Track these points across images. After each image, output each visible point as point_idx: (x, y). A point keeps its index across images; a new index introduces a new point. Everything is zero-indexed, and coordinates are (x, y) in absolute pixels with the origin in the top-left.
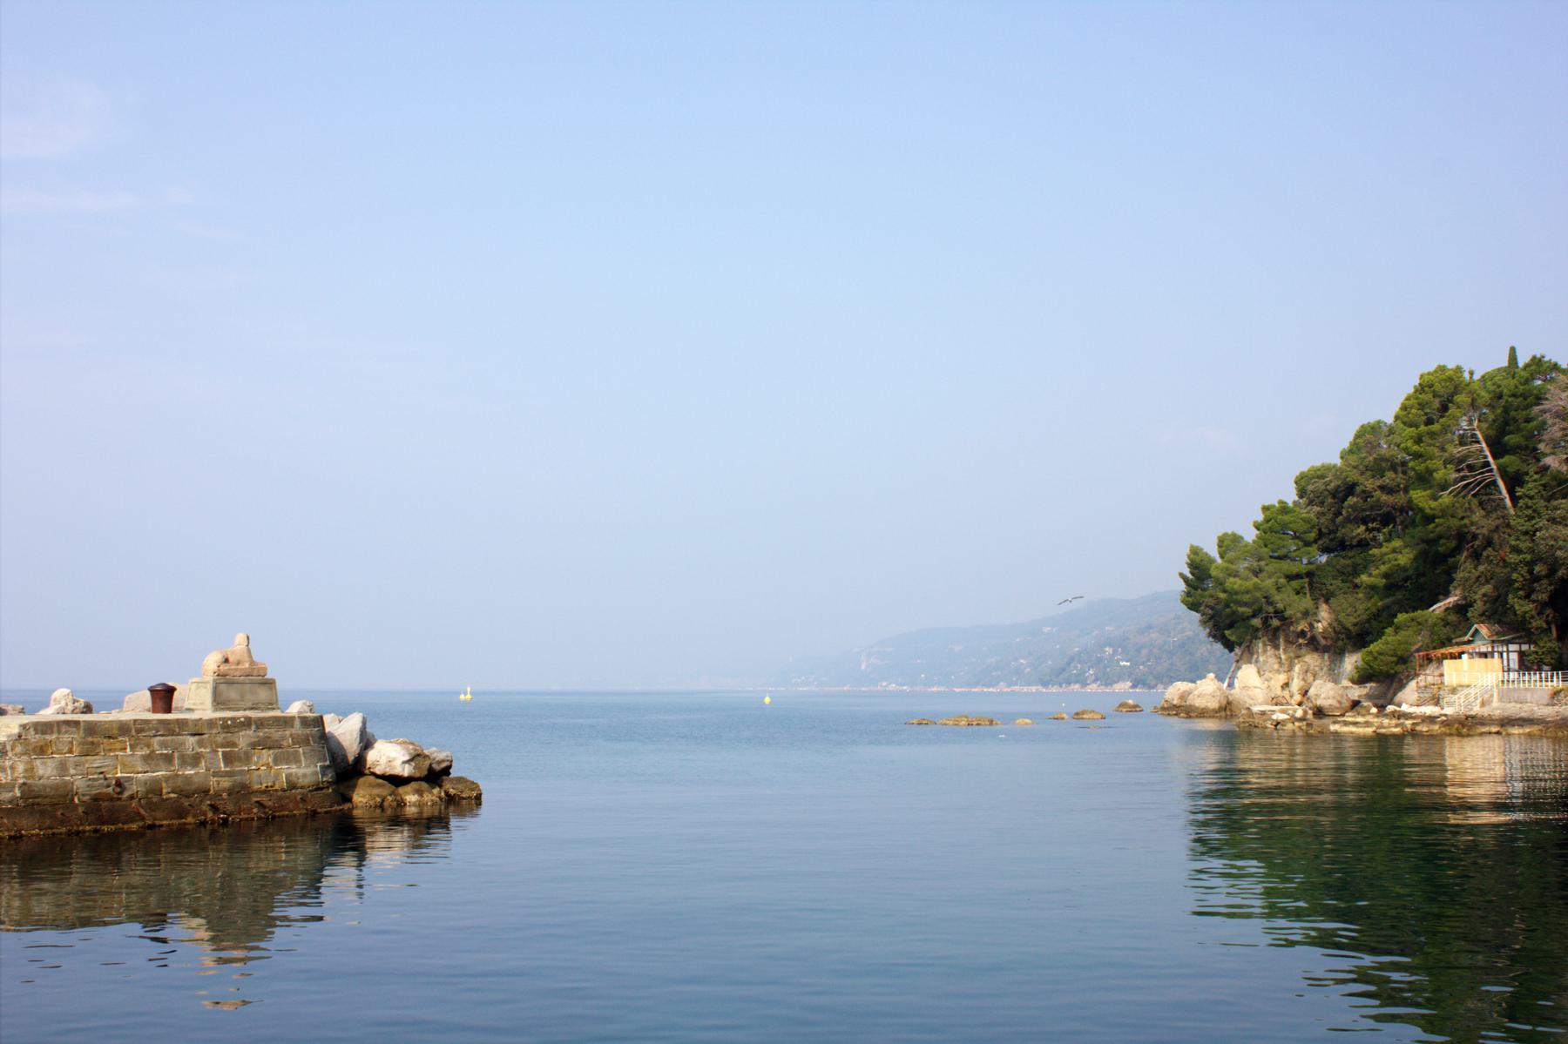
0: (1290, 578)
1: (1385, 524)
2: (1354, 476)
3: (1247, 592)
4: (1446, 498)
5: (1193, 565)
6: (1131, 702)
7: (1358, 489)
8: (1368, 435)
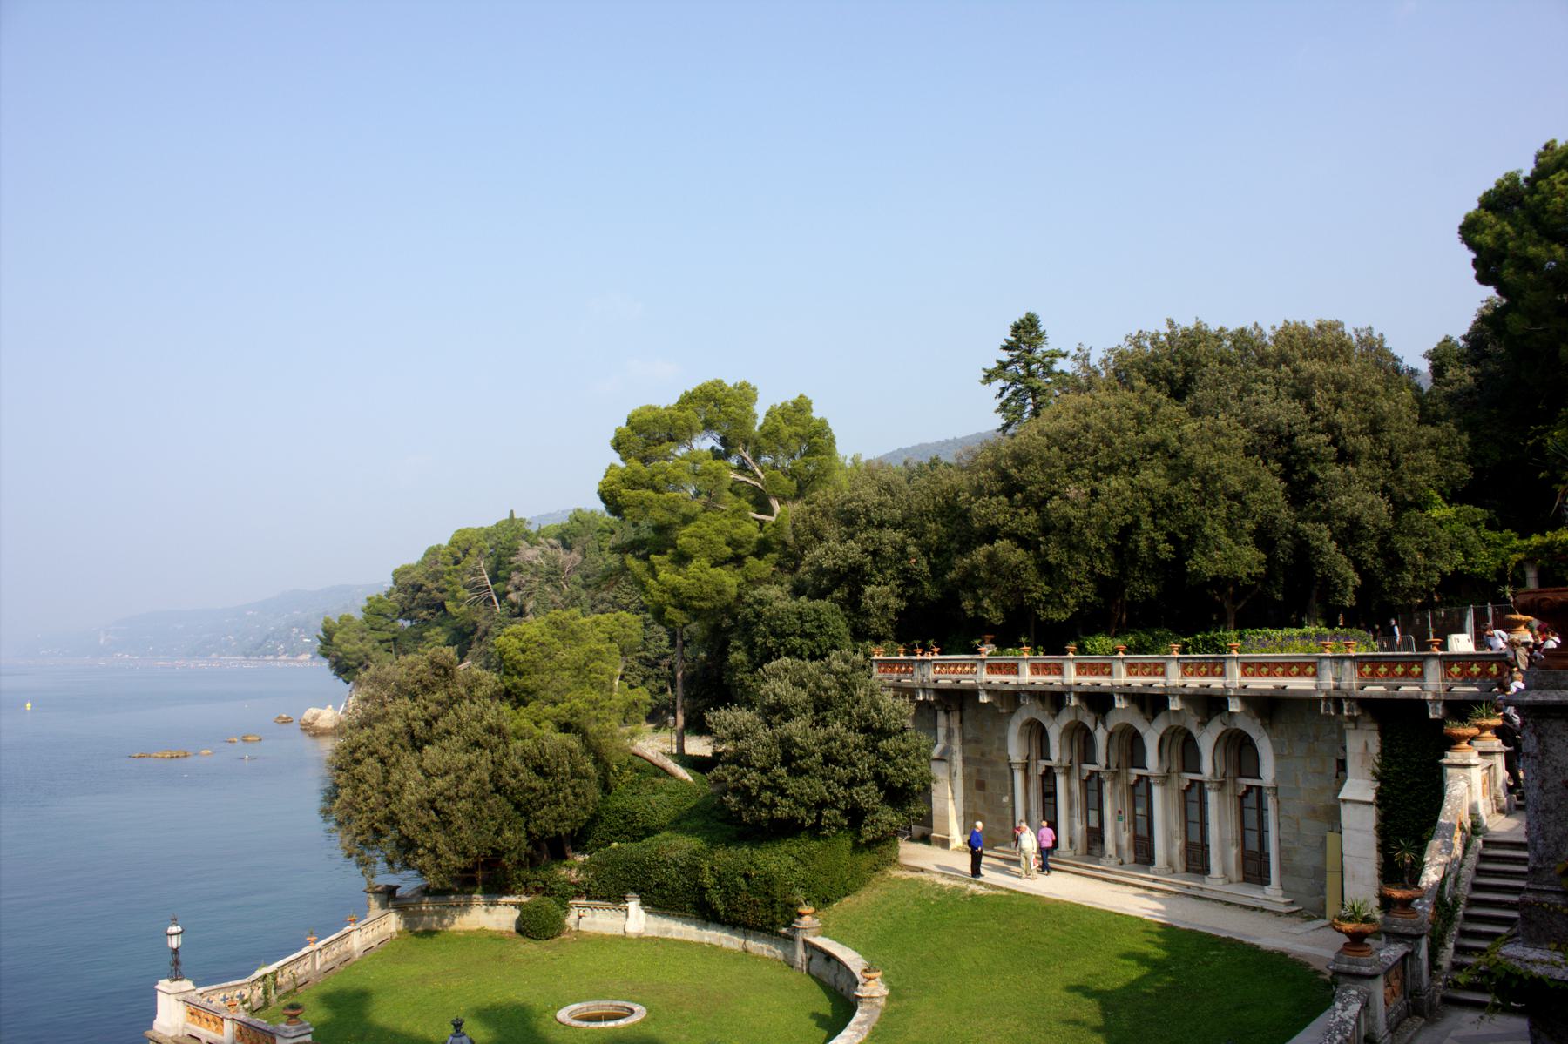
0: (381, 642)
1: (438, 610)
2: (422, 580)
3: (355, 653)
4: (464, 608)
5: (325, 631)
6: (284, 716)
7: (424, 588)
8: (433, 552)
